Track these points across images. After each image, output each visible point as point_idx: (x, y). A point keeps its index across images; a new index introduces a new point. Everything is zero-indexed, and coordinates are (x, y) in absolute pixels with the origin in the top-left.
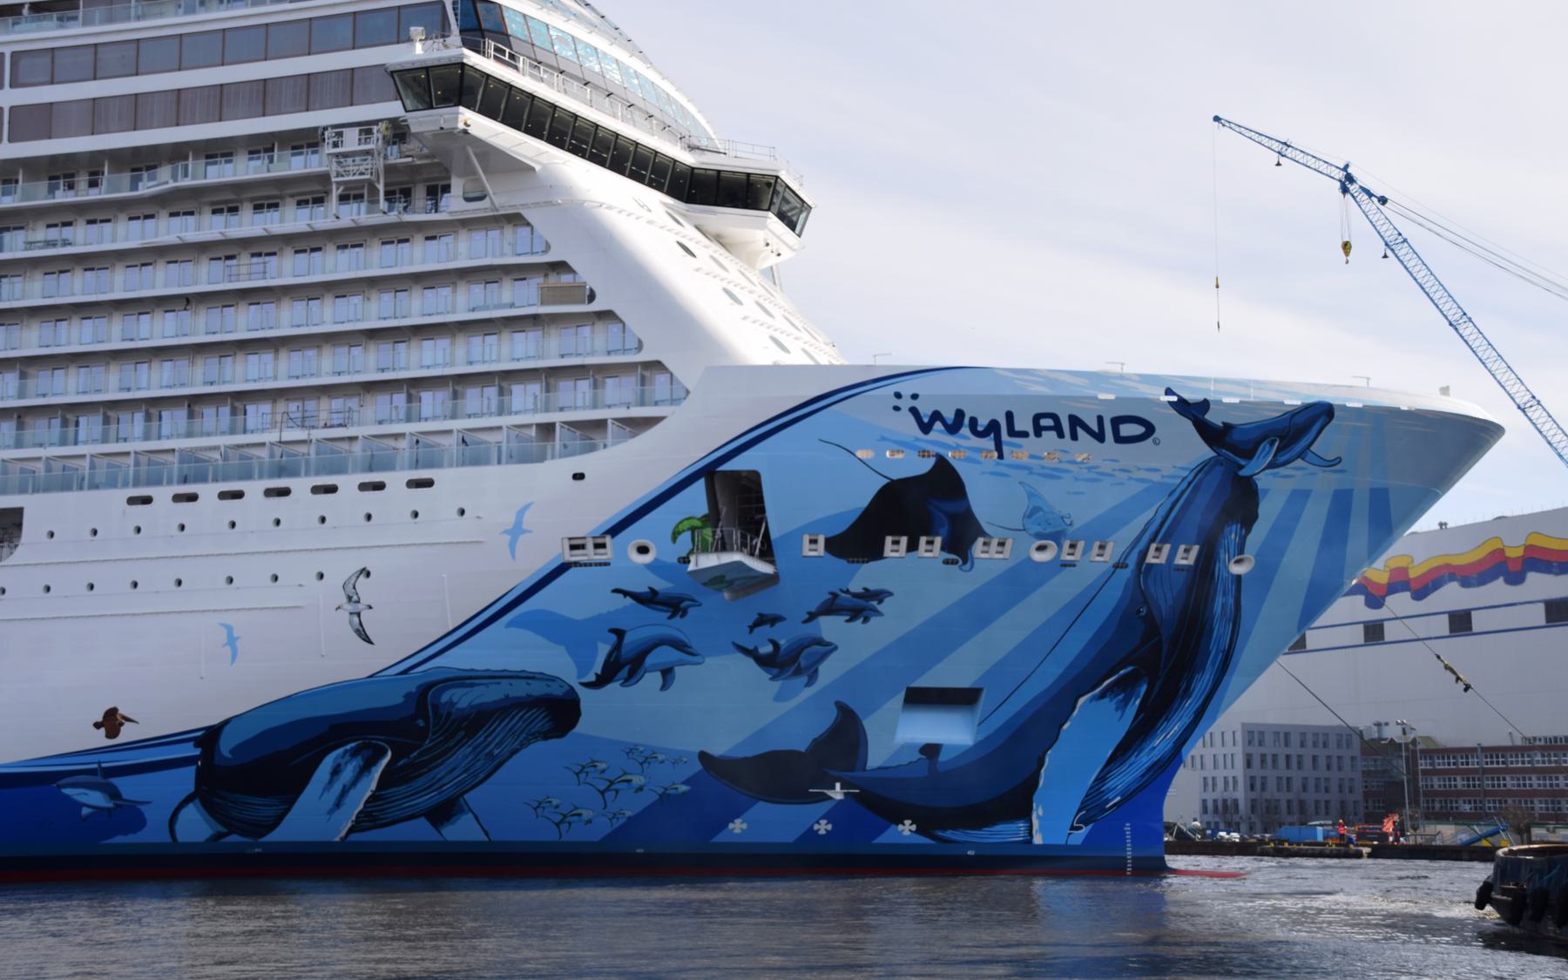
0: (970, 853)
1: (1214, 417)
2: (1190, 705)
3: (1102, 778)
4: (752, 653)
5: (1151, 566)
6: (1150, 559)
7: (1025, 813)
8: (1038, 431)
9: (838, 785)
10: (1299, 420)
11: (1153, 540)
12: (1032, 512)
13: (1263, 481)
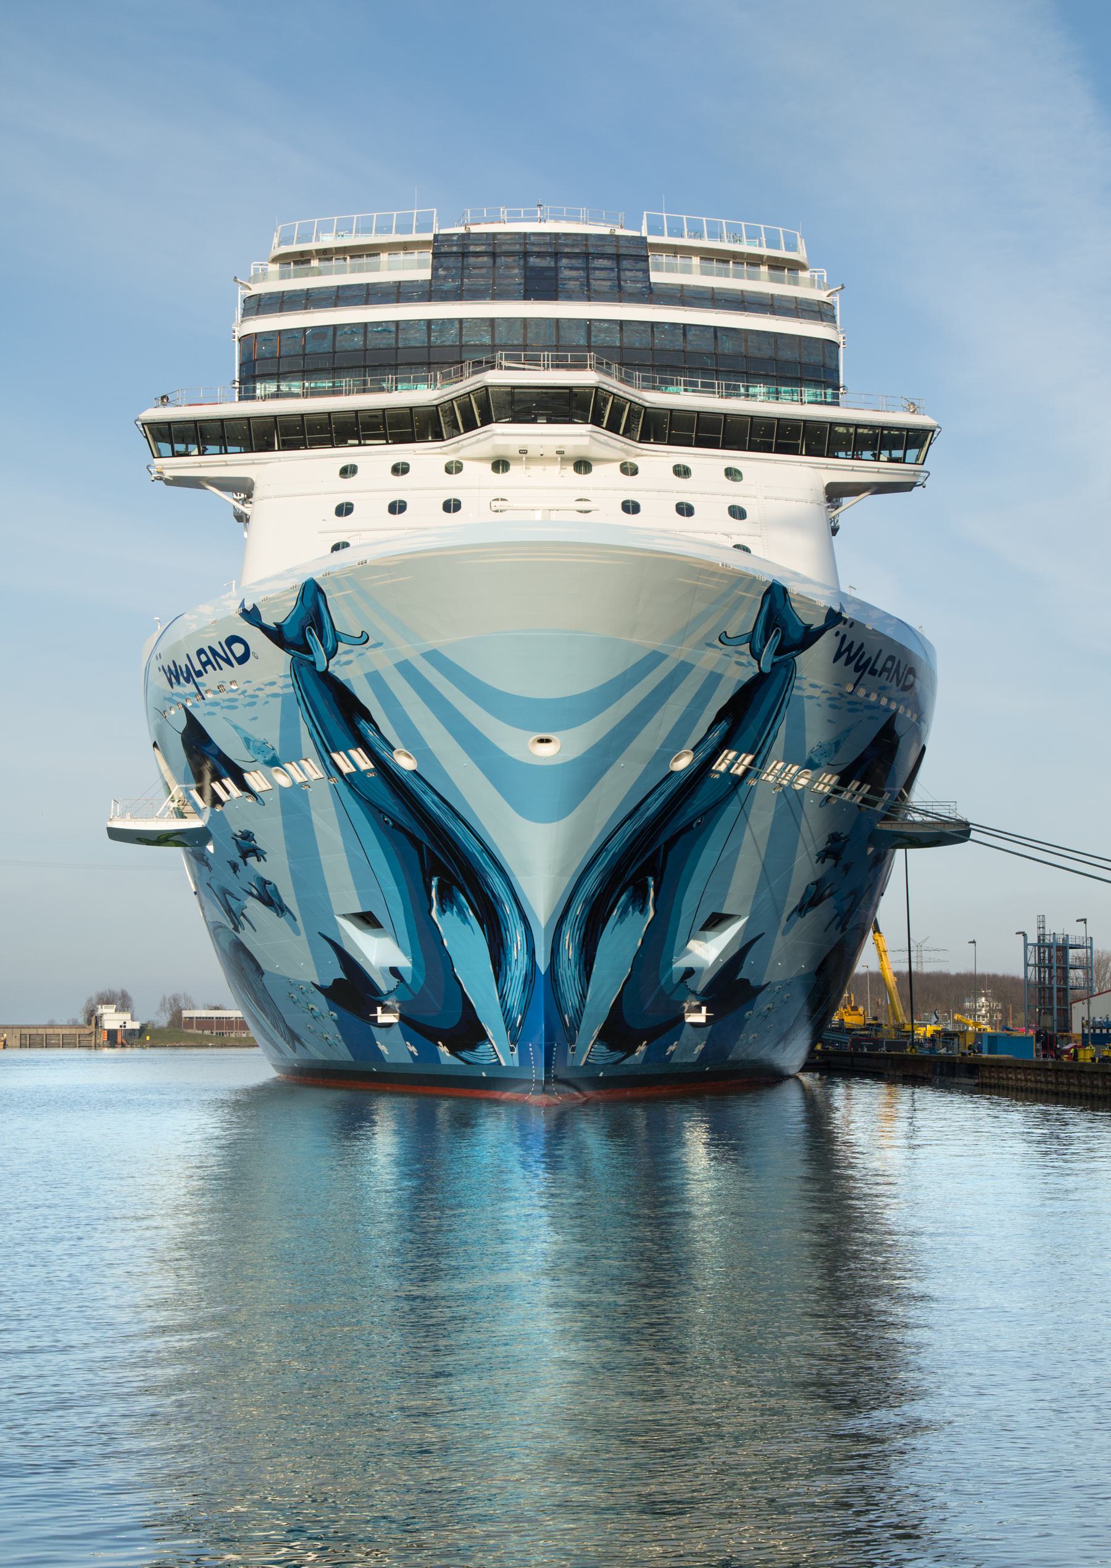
0: (484, 1074)
1: (269, 620)
2: (509, 909)
3: (502, 997)
4: (251, 894)
5: (348, 774)
6: (347, 768)
7: (483, 1037)
8: (204, 665)
9: (379, 1009)
10: (309, 603)
11: (328, 752)
12: (247, 741)
13: (340, 669)
